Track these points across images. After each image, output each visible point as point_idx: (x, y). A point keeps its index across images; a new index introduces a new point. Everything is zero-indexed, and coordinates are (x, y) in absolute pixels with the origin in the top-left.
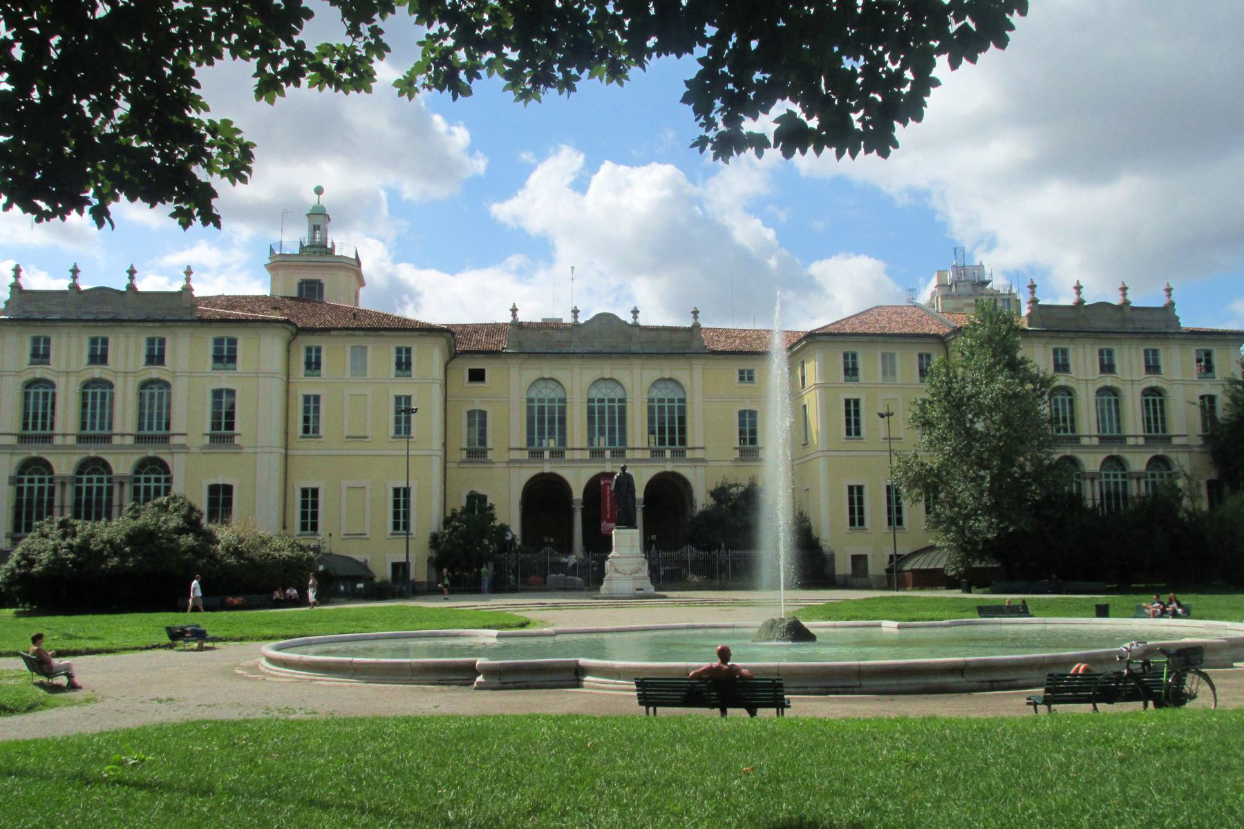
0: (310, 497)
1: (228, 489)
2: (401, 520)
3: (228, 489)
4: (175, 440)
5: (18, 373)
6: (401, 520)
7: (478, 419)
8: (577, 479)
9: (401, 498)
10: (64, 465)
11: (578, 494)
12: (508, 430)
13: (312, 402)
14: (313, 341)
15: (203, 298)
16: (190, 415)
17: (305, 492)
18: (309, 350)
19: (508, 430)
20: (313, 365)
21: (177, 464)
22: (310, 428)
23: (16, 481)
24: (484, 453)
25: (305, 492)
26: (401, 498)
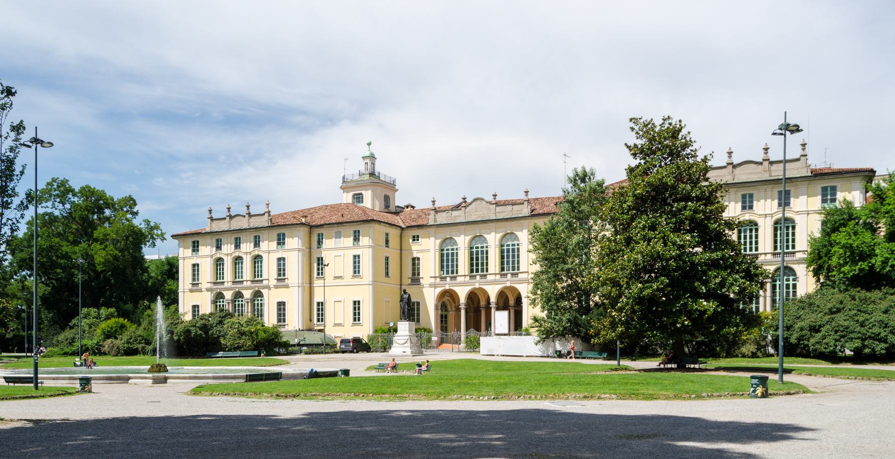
0: (321, 305)
1: (284, 303)
2: (357, 317)
3: (284, 303)
4: (265, 282)
5: (212, 256)
6: (357, 317)
7: (415, 261)
8: (462, 293)
9: (356, 304)
10: (228, 295)
11: (463, 300)
12: (429, 267)
13: (320, 260)
14: (319, 231)
15: (279, 215)
16: (269, 270)
17: (318, 304)
18: (319, 235)
19: (429, 267)
20: (320, 243)
21: (265, 292)
22: (320, 273)
23: (214, 302)
24: (418, 280)
25: (318, 304)
26: (356, 304)
